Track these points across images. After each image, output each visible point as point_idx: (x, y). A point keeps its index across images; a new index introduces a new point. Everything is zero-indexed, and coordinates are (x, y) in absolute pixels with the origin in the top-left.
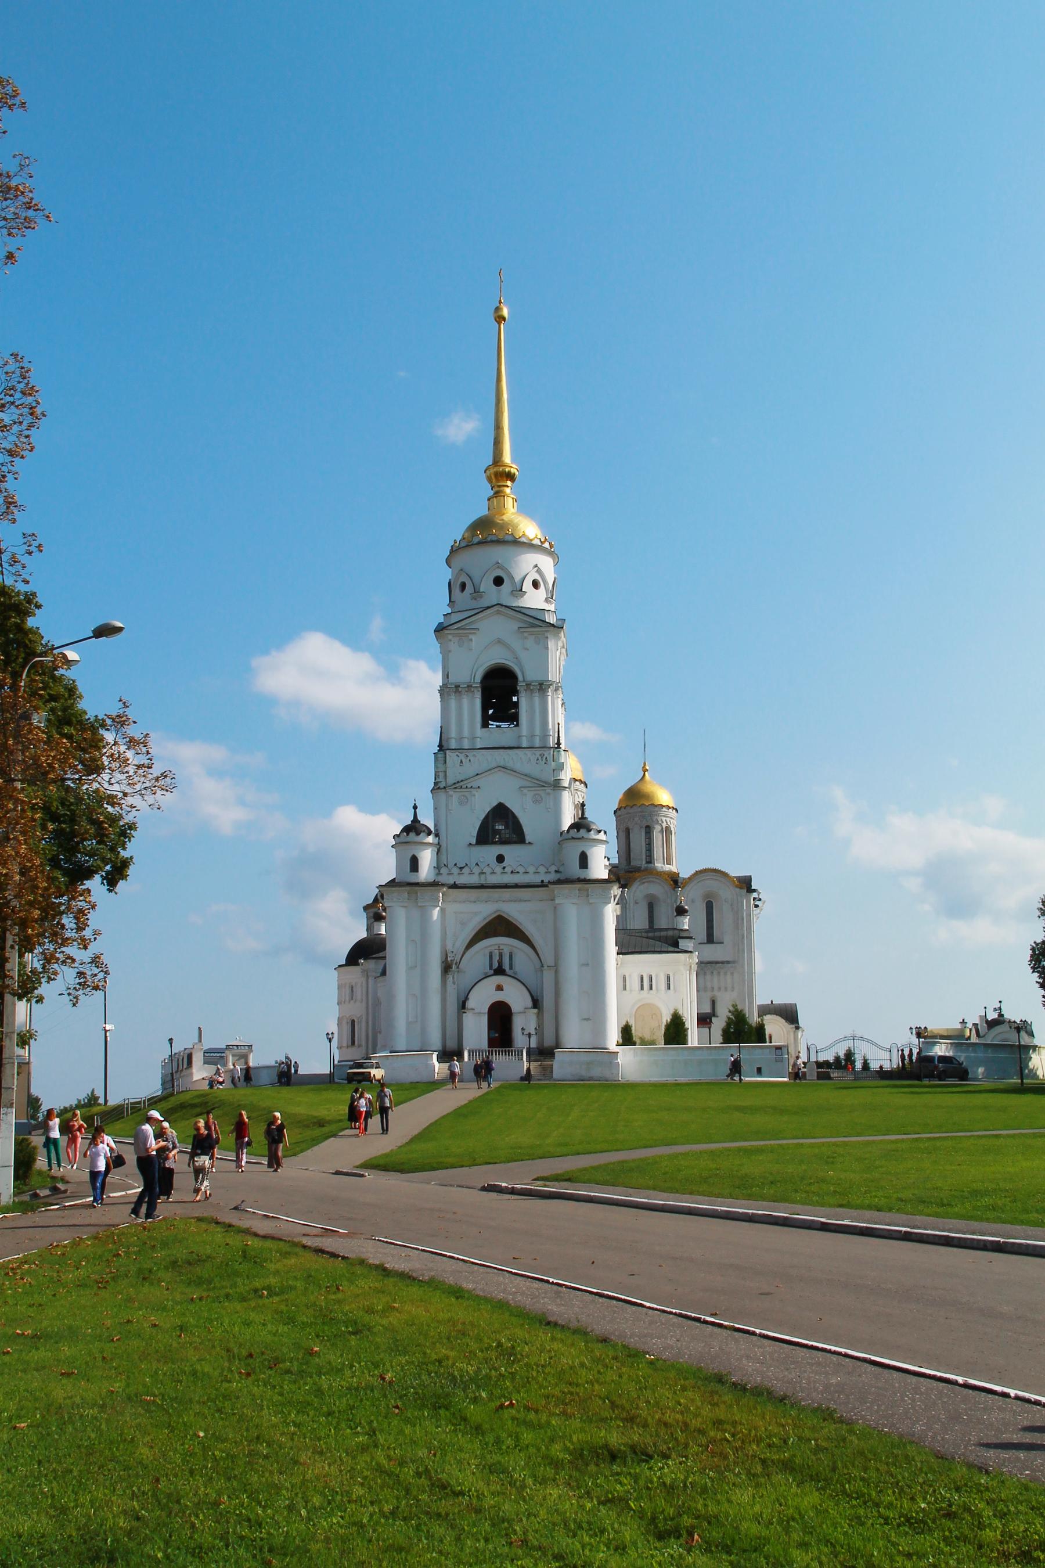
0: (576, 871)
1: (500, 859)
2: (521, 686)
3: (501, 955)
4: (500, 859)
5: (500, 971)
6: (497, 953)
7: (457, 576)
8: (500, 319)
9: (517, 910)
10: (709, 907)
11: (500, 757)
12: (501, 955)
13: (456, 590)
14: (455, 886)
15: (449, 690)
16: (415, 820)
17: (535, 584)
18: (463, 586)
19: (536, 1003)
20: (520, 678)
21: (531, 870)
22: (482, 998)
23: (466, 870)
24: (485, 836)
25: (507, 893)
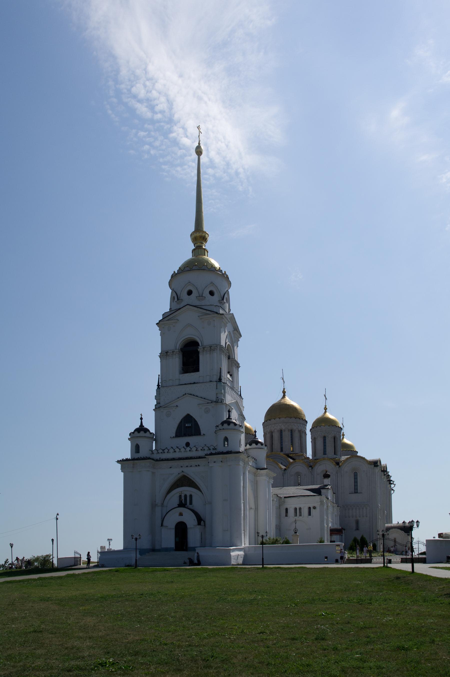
0: (221, 448)
1: (188, 444)
2: (200, 349)
3: (186, 496)
4: (188, 444)
5: (182, 505)
6: (183, 495)
9: (192, 472)
11: (188, 389)
12: (186, 496)
14: (157, 460)
15: (164, 355)
16: (141, 425)
17: (212, 293)
20: (200, 345)
21: (199, 449)
22: (173, 519)
23: (166, 451)
25: (186, 462)
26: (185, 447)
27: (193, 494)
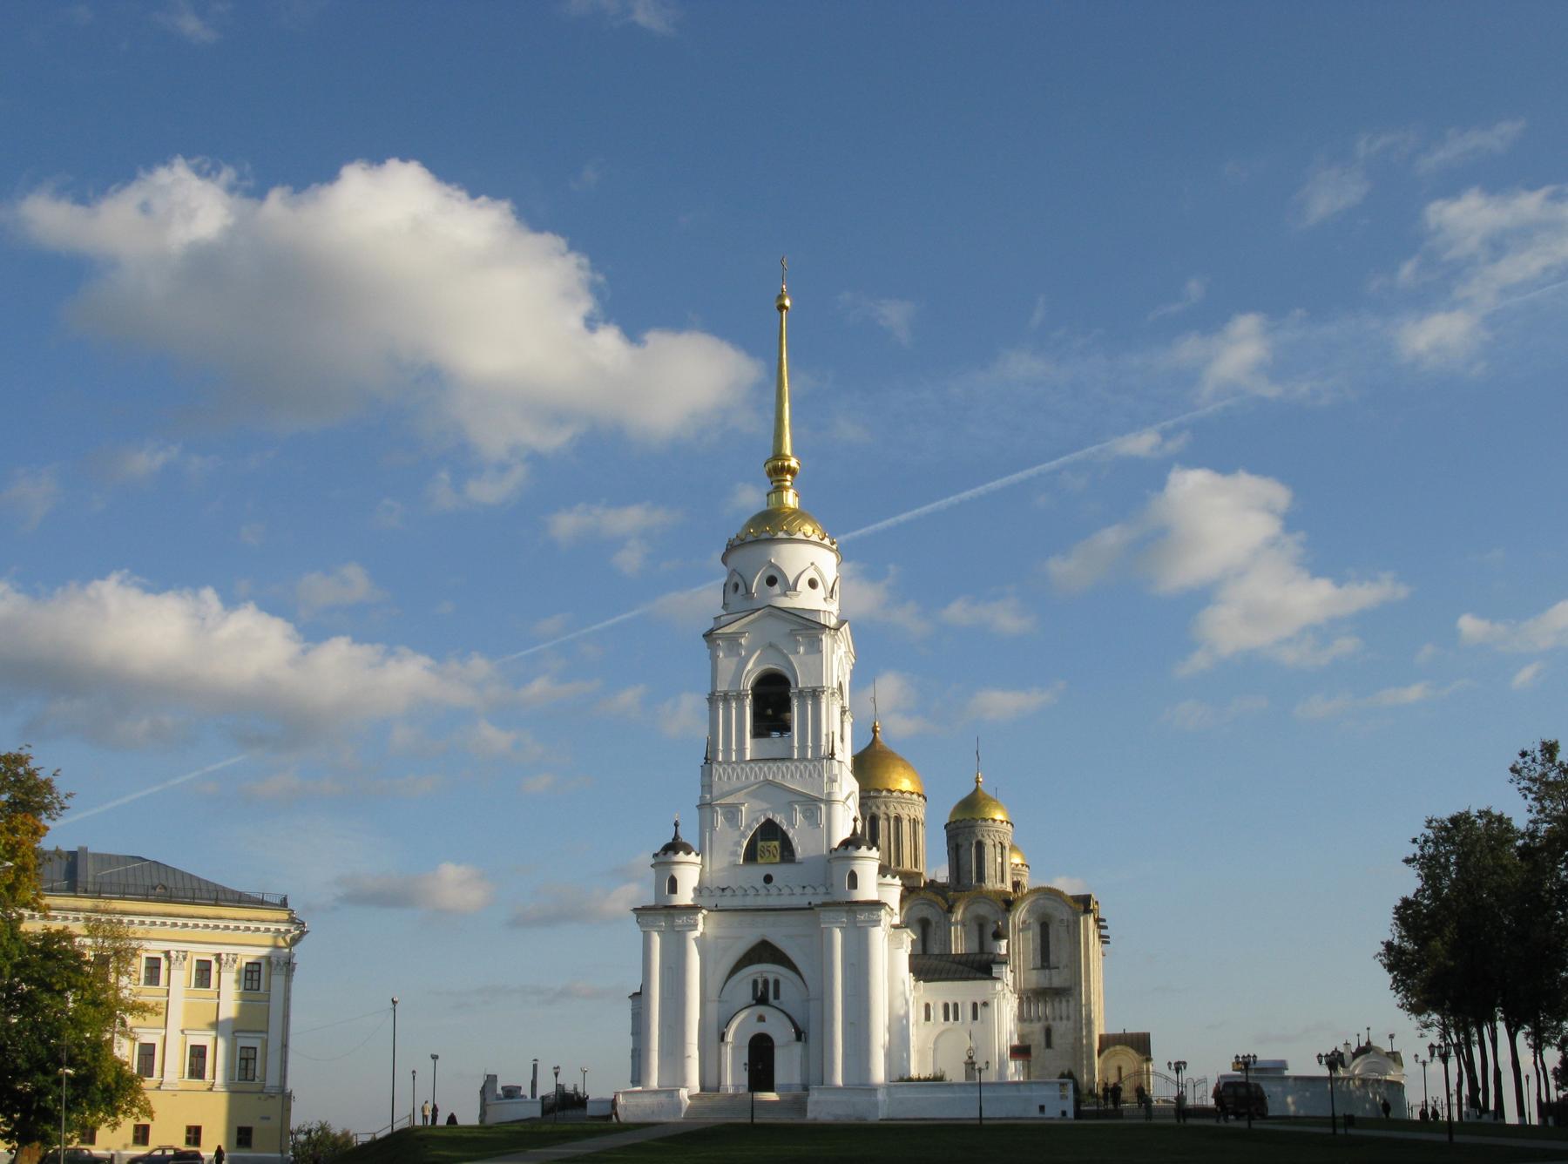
1: (768, 879)
3: (766, 982)
4: (768, 879)
5: (761, 1000)
7: (731, 575)
8: (782, 307)
9: (780, 934)
10: (1044, 927)
12: (766, 982)
13: (731, 588)
16: (676, 837)
17: (813, 584)
18: (736, 587)
19: (800, 1035)
23: (728, 892)
24: (751, 855)
26: (760, 883)
27: (781, 979)
